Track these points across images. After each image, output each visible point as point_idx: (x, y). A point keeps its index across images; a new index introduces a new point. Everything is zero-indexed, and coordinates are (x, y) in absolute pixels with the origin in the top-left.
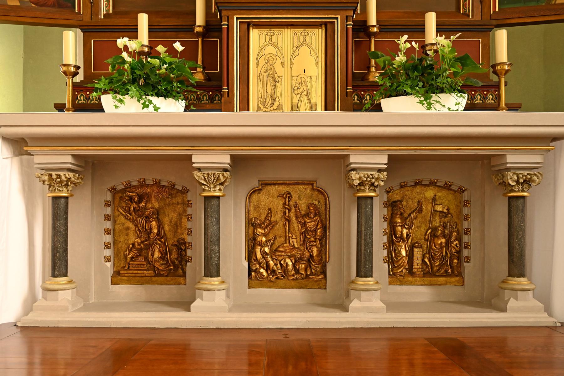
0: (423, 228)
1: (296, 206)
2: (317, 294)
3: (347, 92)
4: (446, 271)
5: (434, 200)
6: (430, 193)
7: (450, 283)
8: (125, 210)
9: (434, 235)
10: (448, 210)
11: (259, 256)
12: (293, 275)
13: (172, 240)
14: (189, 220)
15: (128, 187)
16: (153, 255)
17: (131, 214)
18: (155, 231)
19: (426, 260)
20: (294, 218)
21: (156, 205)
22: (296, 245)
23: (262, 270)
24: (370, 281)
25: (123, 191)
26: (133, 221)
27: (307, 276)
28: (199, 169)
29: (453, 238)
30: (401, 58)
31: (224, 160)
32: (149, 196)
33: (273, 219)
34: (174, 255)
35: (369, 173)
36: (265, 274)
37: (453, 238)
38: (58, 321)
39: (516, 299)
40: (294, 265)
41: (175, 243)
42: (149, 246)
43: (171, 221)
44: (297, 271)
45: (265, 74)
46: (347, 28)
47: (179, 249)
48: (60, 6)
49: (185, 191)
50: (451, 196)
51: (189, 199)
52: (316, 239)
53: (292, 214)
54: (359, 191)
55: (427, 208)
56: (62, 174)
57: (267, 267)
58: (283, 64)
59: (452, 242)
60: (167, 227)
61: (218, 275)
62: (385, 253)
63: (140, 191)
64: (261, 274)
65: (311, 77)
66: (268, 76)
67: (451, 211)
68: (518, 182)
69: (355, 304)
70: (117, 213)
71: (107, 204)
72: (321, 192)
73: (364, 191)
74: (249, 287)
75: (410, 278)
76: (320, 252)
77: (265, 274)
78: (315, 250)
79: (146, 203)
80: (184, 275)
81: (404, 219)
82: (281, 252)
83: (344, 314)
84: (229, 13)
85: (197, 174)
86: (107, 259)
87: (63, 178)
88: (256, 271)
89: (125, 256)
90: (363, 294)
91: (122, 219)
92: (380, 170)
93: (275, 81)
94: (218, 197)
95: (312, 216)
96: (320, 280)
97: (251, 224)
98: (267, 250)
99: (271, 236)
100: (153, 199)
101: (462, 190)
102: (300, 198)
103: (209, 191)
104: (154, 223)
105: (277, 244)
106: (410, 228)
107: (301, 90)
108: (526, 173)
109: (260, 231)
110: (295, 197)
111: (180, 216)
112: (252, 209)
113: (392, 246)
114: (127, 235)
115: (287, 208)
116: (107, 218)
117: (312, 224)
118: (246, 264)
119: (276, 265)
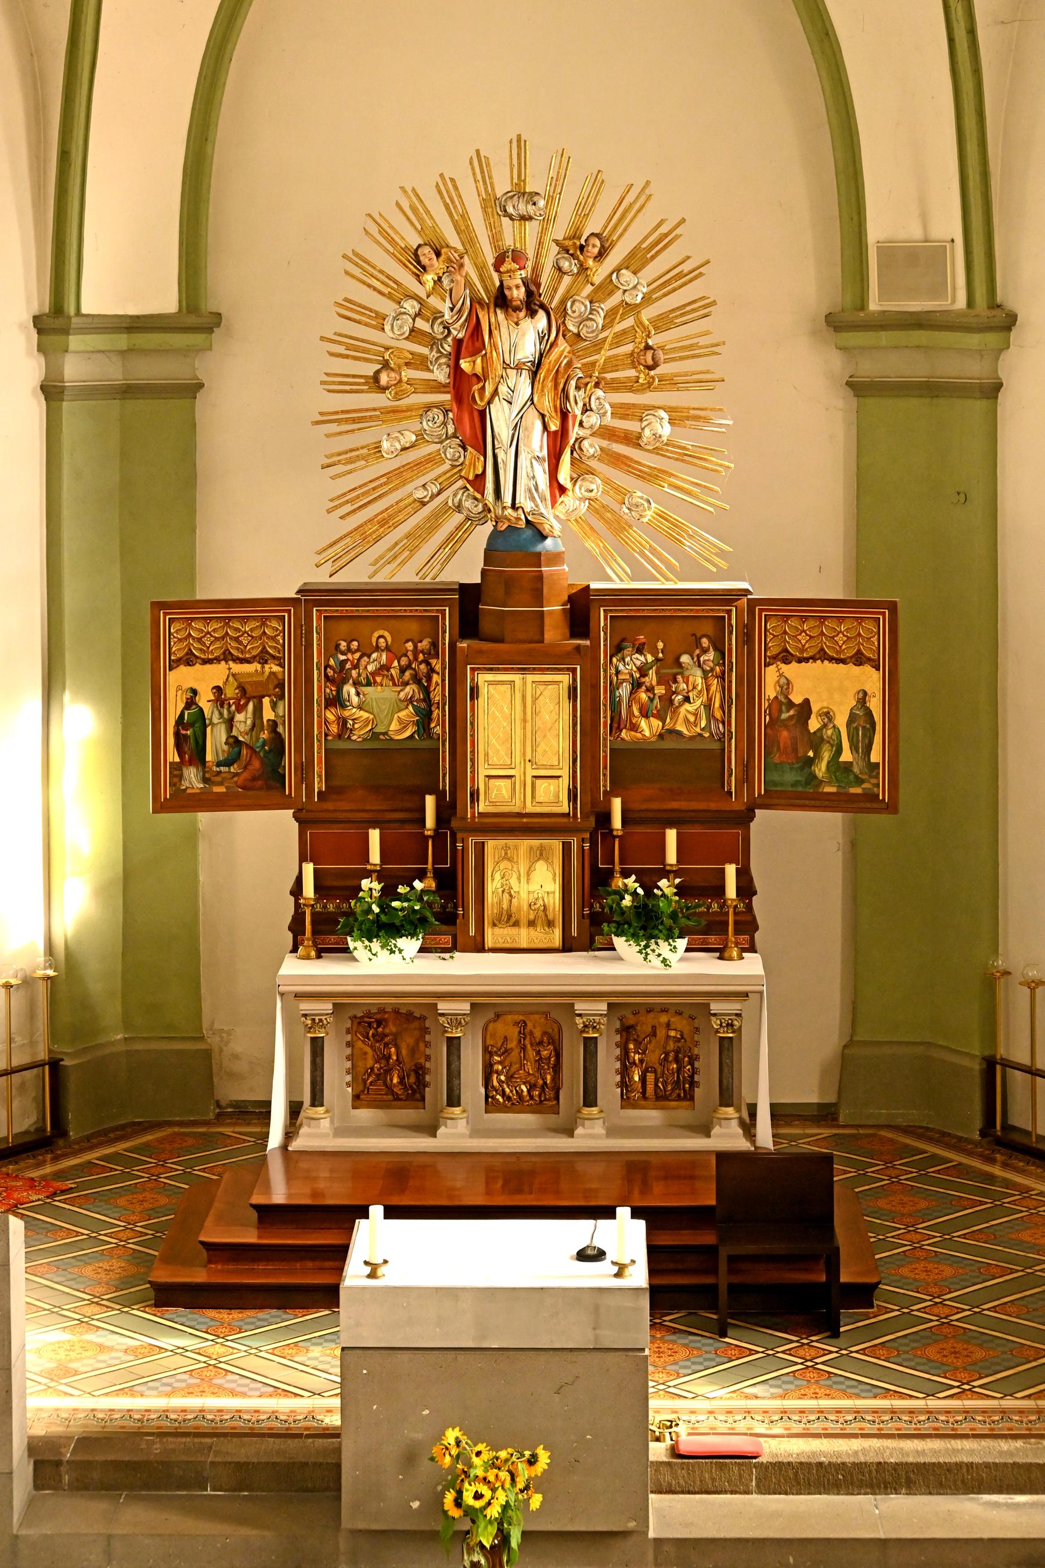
0: (658, 1052)
1: (531, 1033)
2: (551, 1118)
3: (583, 914)
4: (679, 1095)
5: (668, 1025)
6: (664, 1019)
7: (682, 1107)
8: (362, 1035)
9: (666, 1059)
10: (682, 1035)
11: (495, 1083)
12: (528, 1101)
13: (409, 1064)
14: (426, 1046)
16: (391, 1080)
17: (369, 1040)
18: (395, 1058)
19: (660, 1085)
20: (529, 1046)
21: (394, 1030)
22: (531, 1072)
23: (498, 1097)
24: (595, 1110)
25: (362, 1017)
26: (371, 1047)
27: (541, 1101)
28: (443, 1015)
29: (685, 1064)
30: (627, 901)
32: (386, 1020)
33: (509, 1046)
34: (412, 1080)
35: (591, 1018)
36: (501, 1100)
37: (685, 1064)
38: (325, 1147)
39: (721, 1126)
40: (529, 1091)
41: (413, 1067)
42: (388, 1071)
43: (408, 1046)
44: (532, 1098)
45: (500, 890)
46: (583, 850)
47: (416, 1072)
48: (269, 788)
49: (423, 1018)
50: (684, 1022)
51: (427, 1026)
52: (549, 1067)
53: (527, 1042)
54: (582, 1032)
55: (661, 1033)
56: (323, 1018)
57: (503, 1094)
58: (519, 879)
59: (685, 1067)
60: (404, 1052)
61: (459, 1105)
62: (618, 1078)
63: (378, 1016)
64: (498, 1100)
65: (548, 893)
66: (503, 892)
67: (685, 1036)
68: (721, 1025)
69: (579, 1131)
70: (355, 1038)
71: (348, 1032)
72: (556, 1022)
73: (588, 1032)
74: (486, 1112)
75: (643, 1102)
76: (553, 1079)
77: (501, 1100)
78: (549, 1077)
79: (383, 1029)
80: (423, 1099)
81: (638, 1043)
82: (517, 1078)
83: (570, 1140)
84: (464, 835)
85: (442, 1019)
86: (348, 1084)
87: (325, 1022)
88: (493, 1097)
89: (365, 1081)
90: (586, 1122)
91: (360, 1044)
92: (601, 1015)
93: (511, 896)
94: (459, 1038)
95: (546, 1045)
96: (552, 1106)
97: (487, 1052)
98: (503, 1078)
99: (507, 1063)
100: (390, 1024)
101: (692, 1018)
102: (534, 1027)
103: (452, 1032)
104: (393, 1050)
105: (513, 1070)
106: (644, 1053)
107: (538, 906)
108: (727, 1018)
109: (496, 1058)
110: (530, 1025)
111: (417, 1041)
112: (488, 1037)
113: (625, 1072)
114: (365, 1059)
115: (523, 1034)
116: (348, 1044)
117: (546, 1052)
118: (483, 1090)
119: (511, 1091)
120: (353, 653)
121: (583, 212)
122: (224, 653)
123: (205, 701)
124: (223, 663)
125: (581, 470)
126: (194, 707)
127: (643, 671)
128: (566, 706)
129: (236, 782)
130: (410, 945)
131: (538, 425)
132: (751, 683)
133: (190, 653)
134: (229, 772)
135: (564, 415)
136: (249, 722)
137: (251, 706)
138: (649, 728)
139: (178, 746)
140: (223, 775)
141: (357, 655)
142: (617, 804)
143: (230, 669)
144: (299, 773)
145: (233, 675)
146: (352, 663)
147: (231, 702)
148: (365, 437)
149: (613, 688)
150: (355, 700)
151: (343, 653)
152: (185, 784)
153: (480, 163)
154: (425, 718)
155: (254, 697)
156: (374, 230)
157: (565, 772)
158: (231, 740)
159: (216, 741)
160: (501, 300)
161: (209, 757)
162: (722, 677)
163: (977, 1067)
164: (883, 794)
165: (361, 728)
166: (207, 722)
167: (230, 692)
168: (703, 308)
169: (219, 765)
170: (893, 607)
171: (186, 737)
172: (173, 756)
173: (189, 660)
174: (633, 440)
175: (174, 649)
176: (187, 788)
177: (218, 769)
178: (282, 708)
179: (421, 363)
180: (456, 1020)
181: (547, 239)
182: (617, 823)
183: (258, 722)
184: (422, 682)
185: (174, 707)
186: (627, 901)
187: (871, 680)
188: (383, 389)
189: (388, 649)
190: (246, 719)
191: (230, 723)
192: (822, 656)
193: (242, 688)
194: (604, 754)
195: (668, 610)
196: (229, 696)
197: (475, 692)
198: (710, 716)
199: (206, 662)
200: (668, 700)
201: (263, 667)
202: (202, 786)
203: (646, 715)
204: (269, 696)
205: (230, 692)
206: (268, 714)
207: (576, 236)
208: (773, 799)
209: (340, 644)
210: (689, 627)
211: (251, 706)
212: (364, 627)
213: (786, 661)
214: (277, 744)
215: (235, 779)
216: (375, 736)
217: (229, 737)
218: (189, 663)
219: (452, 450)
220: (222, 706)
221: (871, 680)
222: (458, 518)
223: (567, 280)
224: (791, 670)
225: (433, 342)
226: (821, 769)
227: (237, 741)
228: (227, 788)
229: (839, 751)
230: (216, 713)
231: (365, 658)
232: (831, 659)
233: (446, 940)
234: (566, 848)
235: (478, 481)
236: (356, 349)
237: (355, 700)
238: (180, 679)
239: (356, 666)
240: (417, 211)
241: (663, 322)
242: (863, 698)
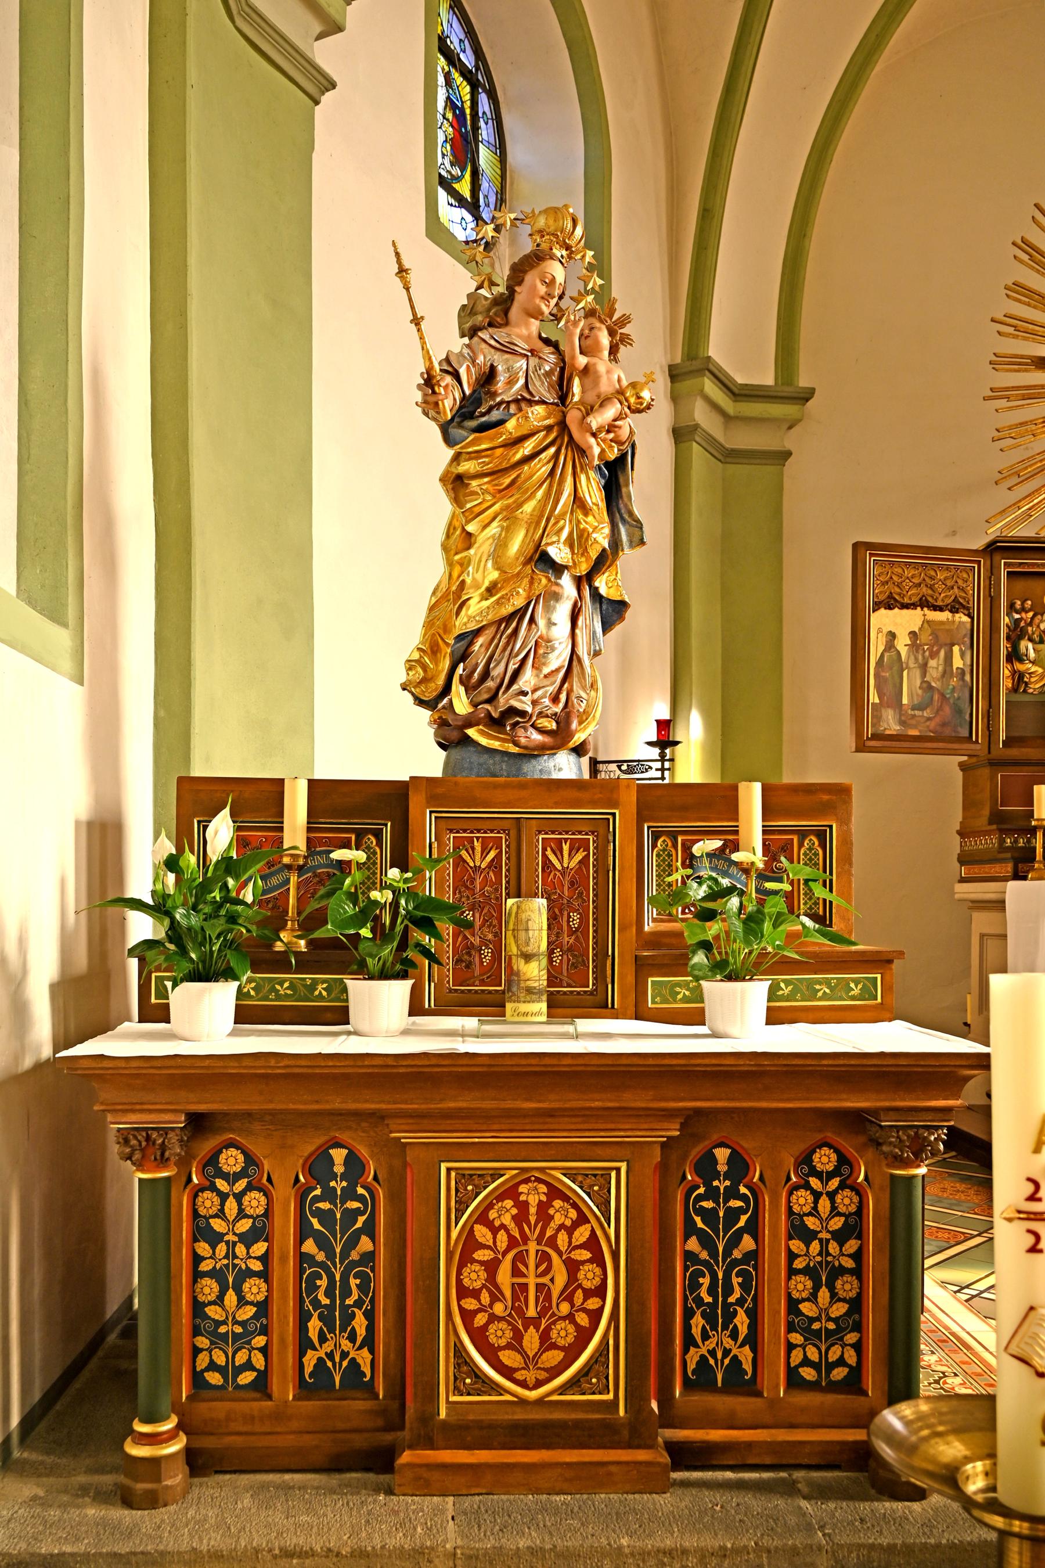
120: (1027, 612)
122: (921, 599)
123: (902, 644)
124: (919, 608)
126: (893, 650)
129: (928, 727)
133: (891, 596)
134: (923, 716)
136: (941, 668)
137: (942, 653)
140: (917, 719)
141: (1031, 614)
143: (924, 615)
144: (986, 720)
145: (928, 622)
146: (1025, 621)
147: (926, 647)
150: (1032, 654)
151: (1017, 612)
155: (946, 645)
158: (925, 685)
161: (905, 701)
165: (1036, 682)
166: (904, 666)
167: (925, 638)
169: (913, 709)
171: (886, 680)
172: (874, 698)
173: (890, 603)
175: (876, 591)
176: (885, 729)
177: (913, 713)
183: (948, 669)
190: (938, 665)
191: (924, 668)
196: (923, 641)
199: (905, 606)
201: (953, 616)
202: (898, 728)
204: (958, 645)
206: (958, 662)
209: (1015, 603)
211: (942, 653)
215: (928, 723)
217: (923, 682)
218: (890, 607)
220: (917, 651)
227: (930, 688)
228: (920, 731)
230: (912, 657)
231: (1039, 617)
237: (1032, 654)
239: (1031, 624)
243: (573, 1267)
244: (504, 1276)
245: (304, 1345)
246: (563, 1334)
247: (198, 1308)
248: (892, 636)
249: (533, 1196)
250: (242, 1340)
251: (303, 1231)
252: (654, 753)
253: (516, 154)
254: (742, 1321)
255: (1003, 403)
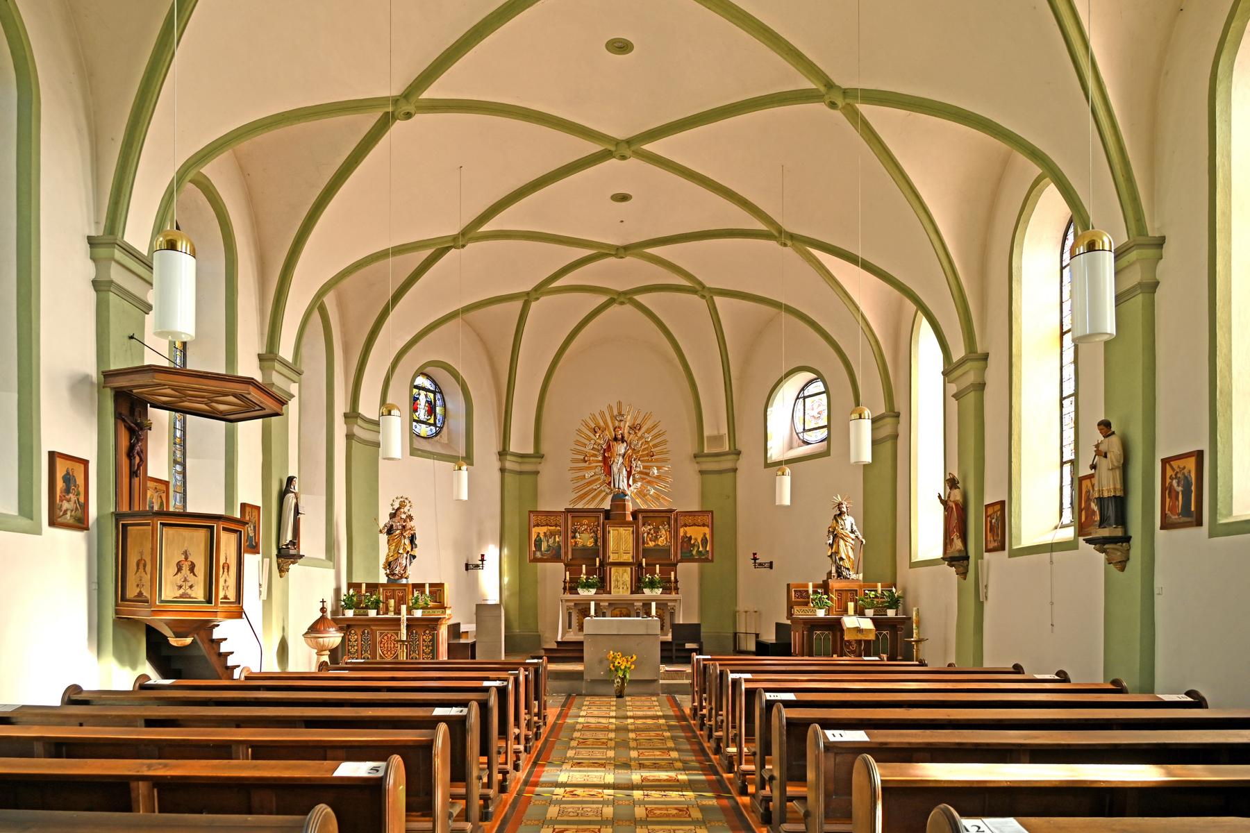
15: (582, 609)
30: (647, 580)
31: (607, 604)
121: (635, 419)
125: (634, 481)
127: (650, 530)
128: (631, 536)
130: (593, 591)
131: (624, 469)
132: (677, 532)
135: (631, 467)
138: (651, 544)
139: (535, 546)
142: (644, 560)
148: (581, 474)
149: (643, 534)
152: (537, 556)
153: (610, 408)
154: (596, 541)
156: (584, 424)
157: (631, 552)
159: (544, 546)
160: (616, 439)
162: (670, 531)
163: (732, 635)
164: (710, 558)
167: (548, 533)
168: (665, 442)
170: (712, 512)
172: (534, 549)
173: (538, 525)
174: (647, 474)
178: (561, 538)
179: (595, 456)
180: (605, 608)
181: (627, 426)
182: (644, 564)
184: (595, 532)
185: (534, 537)
186: (647, 580)
187: (707, 530)
188: (586, 462)
189: (587, 525)
191: (548, 541)
192: (695, 525)
193: (551, 533)
194: (641, 549)
195: (656, 514)
197: (609, 532)
198: (667, 541)
200: (656, 537)
203: (651, 541)
205: (548, 533)
206: (557, 539)
207: (634, 425)
208: (681, 561)
210: (662, 519)
212: (581, 519)
213: (686, 527)
214: (559, 547)
216: (583, 546)
219: (603, 477)
221: (707, 530)
222: (605, 493)
223: (631, 436)
224: (687, 529)
225: (598, 451)
226: (694, 552)
229: (699, 548)
232: (696, 525)
233: (602, 591)
234: (632, 569)
235: (610, 482)
236: (579, 452)
238: (535, 530)
239: (579, 529)
240: (594, 418)
241: (655, 446)
242: (705, 535)
243: (394, 644)
244: (386, 645)
245: (362, 655)
246: (393, 652)
247: (349, 650)
248: (539, 533)
249: (389, 636)
250: (354, 654)
251: (362, 641)
252: (481, 562)
253: (449, 406)
254: (417, 652)
255: (574, 471)
